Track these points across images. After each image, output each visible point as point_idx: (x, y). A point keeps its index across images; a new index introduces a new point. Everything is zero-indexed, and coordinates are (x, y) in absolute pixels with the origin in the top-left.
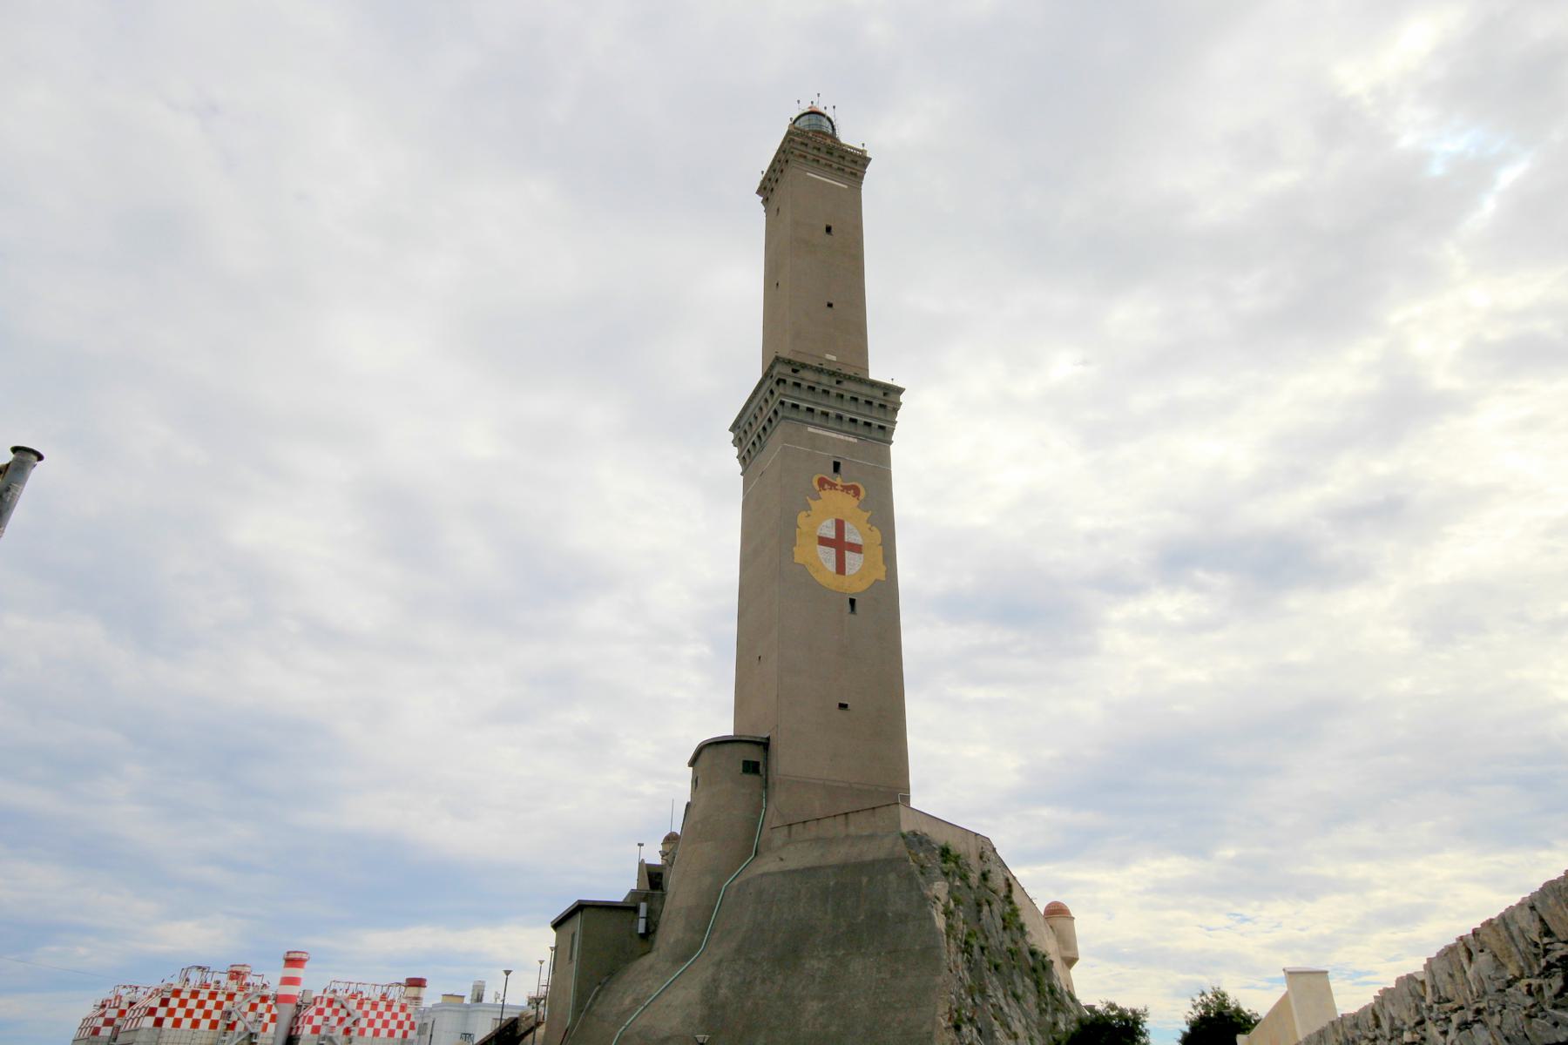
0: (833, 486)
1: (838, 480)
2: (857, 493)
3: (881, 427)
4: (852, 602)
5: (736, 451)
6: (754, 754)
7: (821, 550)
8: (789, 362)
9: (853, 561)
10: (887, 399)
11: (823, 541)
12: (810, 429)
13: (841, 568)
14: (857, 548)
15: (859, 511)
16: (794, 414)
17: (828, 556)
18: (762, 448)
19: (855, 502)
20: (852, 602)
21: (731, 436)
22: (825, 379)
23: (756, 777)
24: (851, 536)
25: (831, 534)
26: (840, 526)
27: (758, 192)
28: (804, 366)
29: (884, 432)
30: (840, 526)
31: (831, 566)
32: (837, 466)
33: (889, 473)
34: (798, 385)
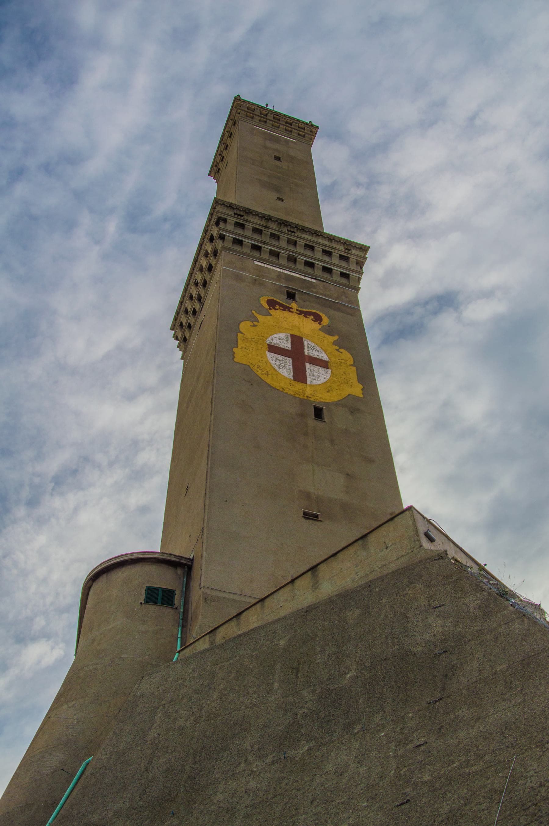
1: (294, 305)
3: (343, 275)
6: (164, 579)
7: (271, 357)
8: (231, 206)
13: (300, 375)
15: (322, 334)
16: (237, 248)
18: (202, 305)
19: (316, 326)
22: (274, 226)
23: (168, 611)
25: (288, 345)
26: (297, 341)
28: (248, 212)
29: (350, 280)
32: (291, 296)
33: (359, 310)
34: (242, 226)
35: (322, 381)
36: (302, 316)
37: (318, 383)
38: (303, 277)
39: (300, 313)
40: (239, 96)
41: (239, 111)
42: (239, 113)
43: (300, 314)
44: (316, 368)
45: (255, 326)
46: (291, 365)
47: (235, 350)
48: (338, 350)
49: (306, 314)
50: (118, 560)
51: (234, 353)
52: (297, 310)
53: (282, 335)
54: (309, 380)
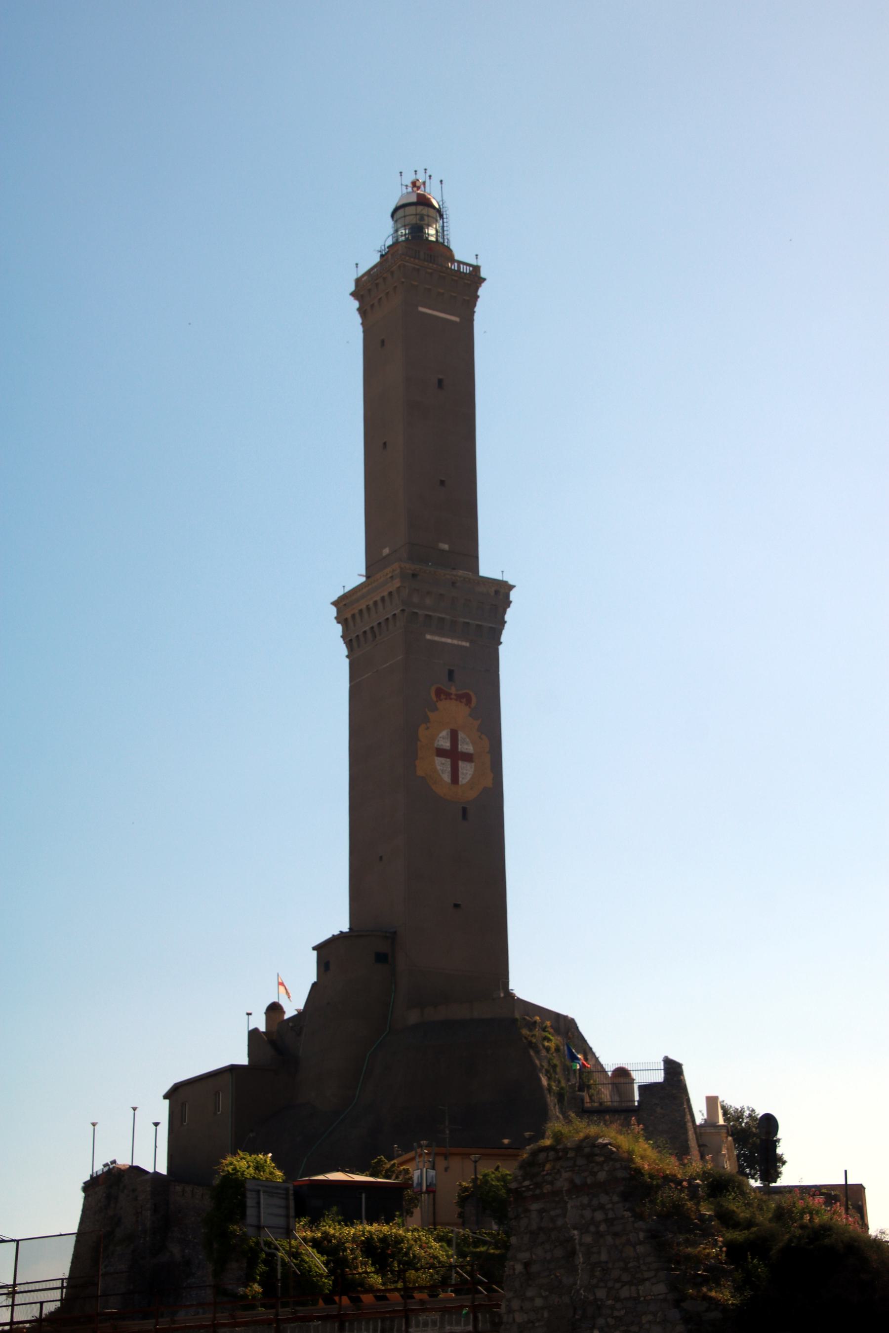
0: (448, 696)
2: (469, 702)
4: (464, 810)
5: (339, 629)
9: (466, 771)
10: (498, 595)
11: (441, 753)
12: (428, 637)
14: (468, 758)
17: (443, 766)
20: (464, 810)
21: (333, 611)
24: (466, 747)
25: (447, 745)
27: (353, 294)
30: (454, 737)
31: (447, 777)
35: (469, 777)
37: (467, 780)
38: (460, 643)
43: (456, 700)
45: (427, 728)
46: (449, 766)
52: (456, 695)
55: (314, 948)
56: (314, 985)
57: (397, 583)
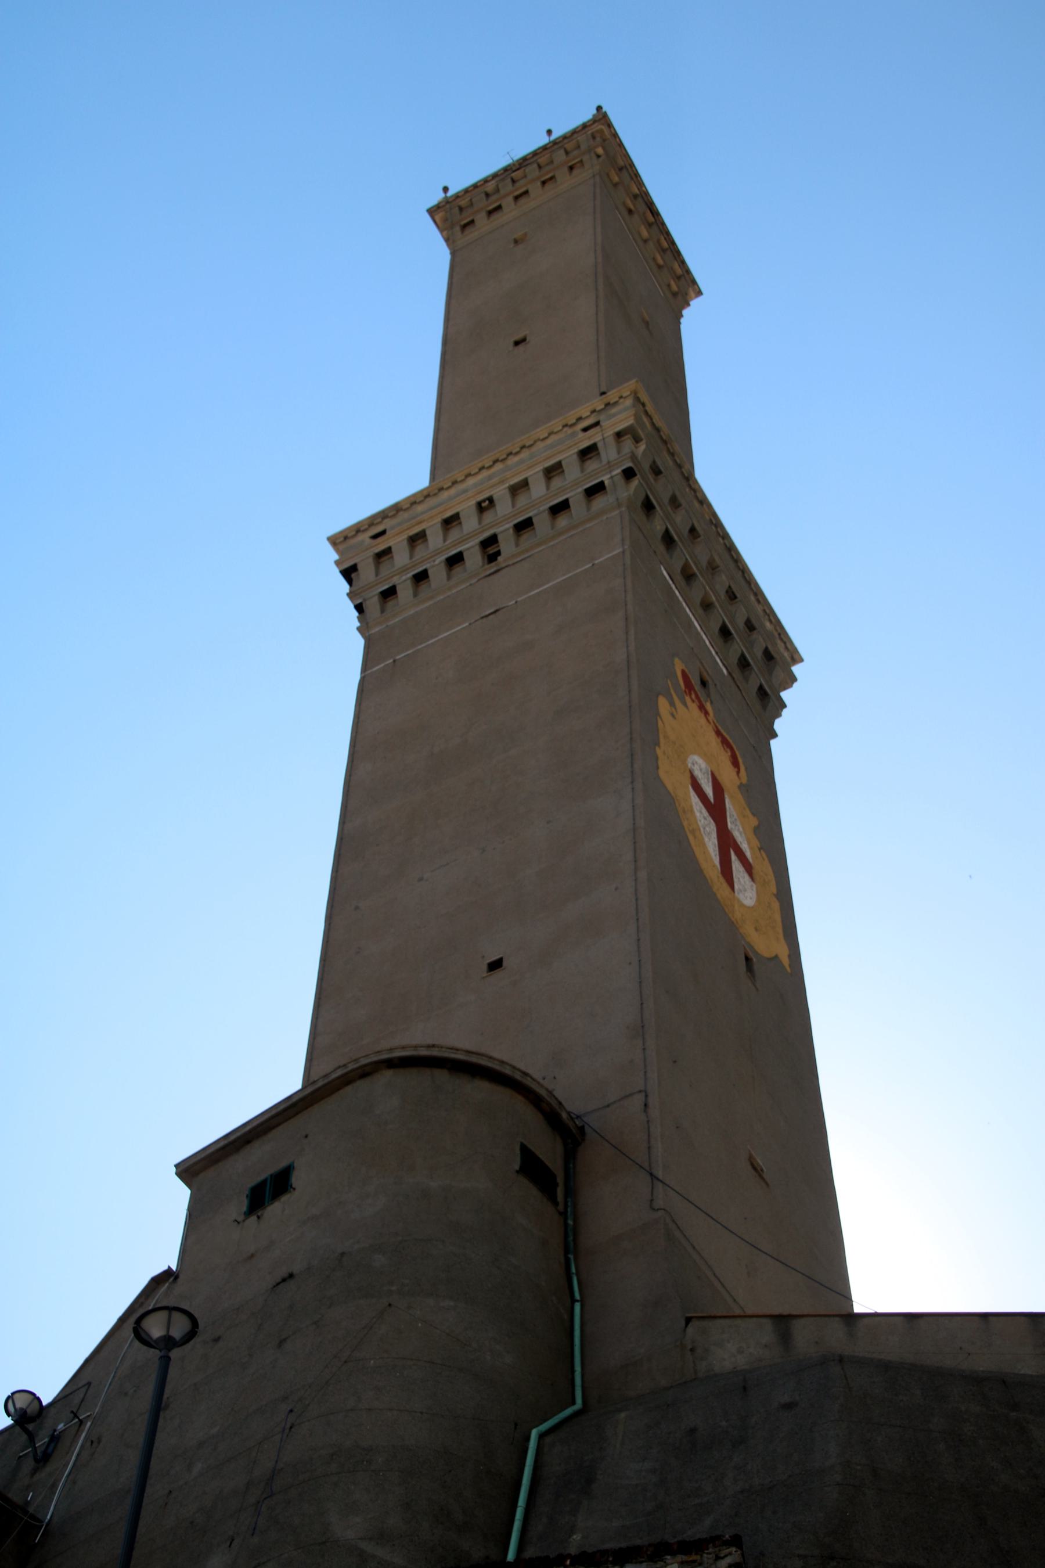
0: (702, 707)
7: (695, 799)
12: (665, 573)
25: (709, 791)
32: (704, 683)
36: (719, 740)
39: (718, 733)
40: (599, 108)
41: (600, 151)
42: (598, 156)
44: (742, 869)
47: (659, 751)
48: (760, 849)
49: (725, 742)
50: (474, 1059)
51: (657, 758)
53: (703, 765)
54: (736, 887)
55: (188, 1171)
56: (162, 1280)
57: (622, 418)
